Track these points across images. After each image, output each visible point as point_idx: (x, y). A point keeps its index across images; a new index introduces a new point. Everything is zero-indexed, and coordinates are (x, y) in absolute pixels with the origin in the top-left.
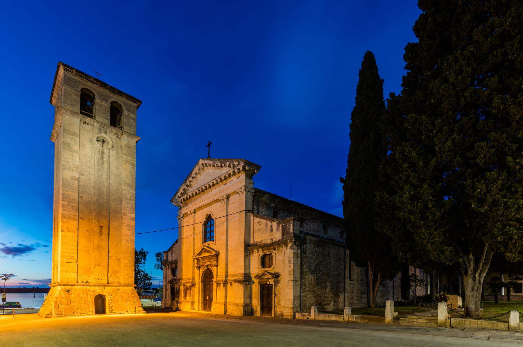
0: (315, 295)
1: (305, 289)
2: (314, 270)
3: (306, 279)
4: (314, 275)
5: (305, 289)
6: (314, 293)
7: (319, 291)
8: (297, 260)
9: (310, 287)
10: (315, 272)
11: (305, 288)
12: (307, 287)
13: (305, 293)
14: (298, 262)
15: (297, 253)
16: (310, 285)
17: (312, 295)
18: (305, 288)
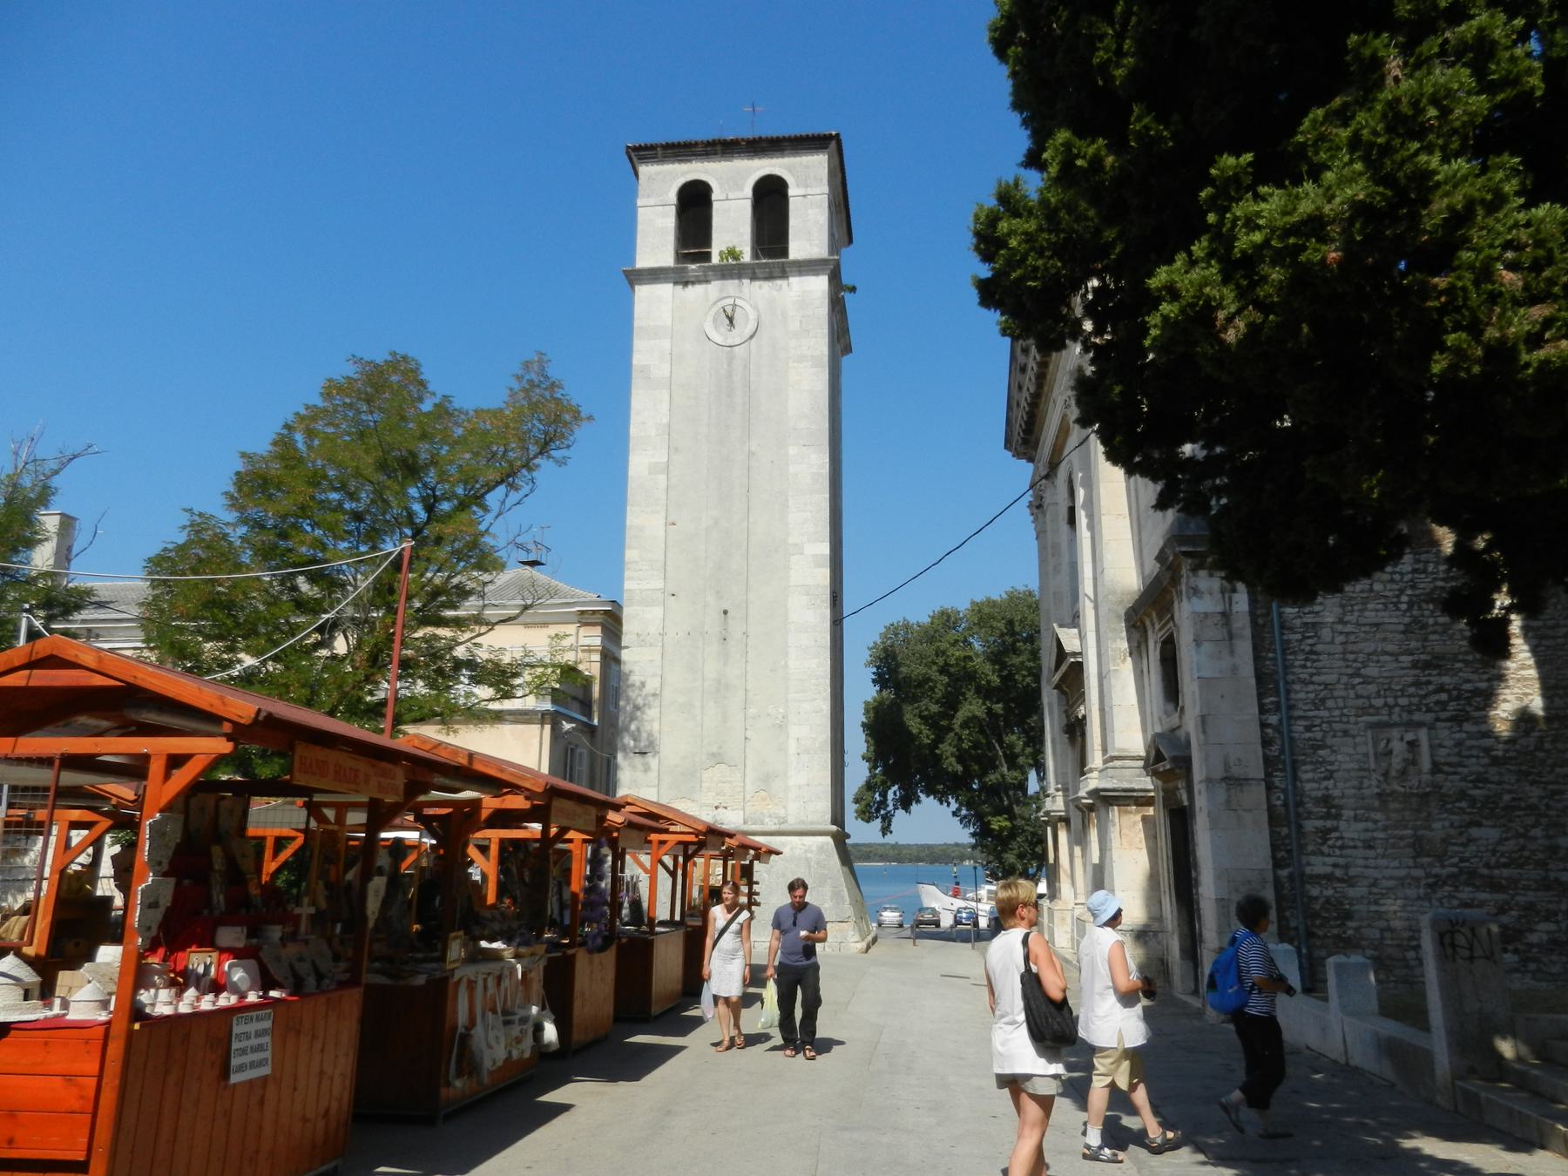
0: (1436, 870)
1: (1336, 829)
2: (1403, 701)
3: (1332, 763)
4: (1410, 736)
5: (1336, 829)
6: (1418, 855)
7: (1470, 840)
8: (1232, 653)
9: (1378, 816)
10: (1417, 717)
11: (1329, 824)
12: (1347, 813)
13: (1330, 860)
14: (1234, 669)
15: (1226, 616)
16: (1377, 804)
17: (1402, 873)
18: (1329, 824)
